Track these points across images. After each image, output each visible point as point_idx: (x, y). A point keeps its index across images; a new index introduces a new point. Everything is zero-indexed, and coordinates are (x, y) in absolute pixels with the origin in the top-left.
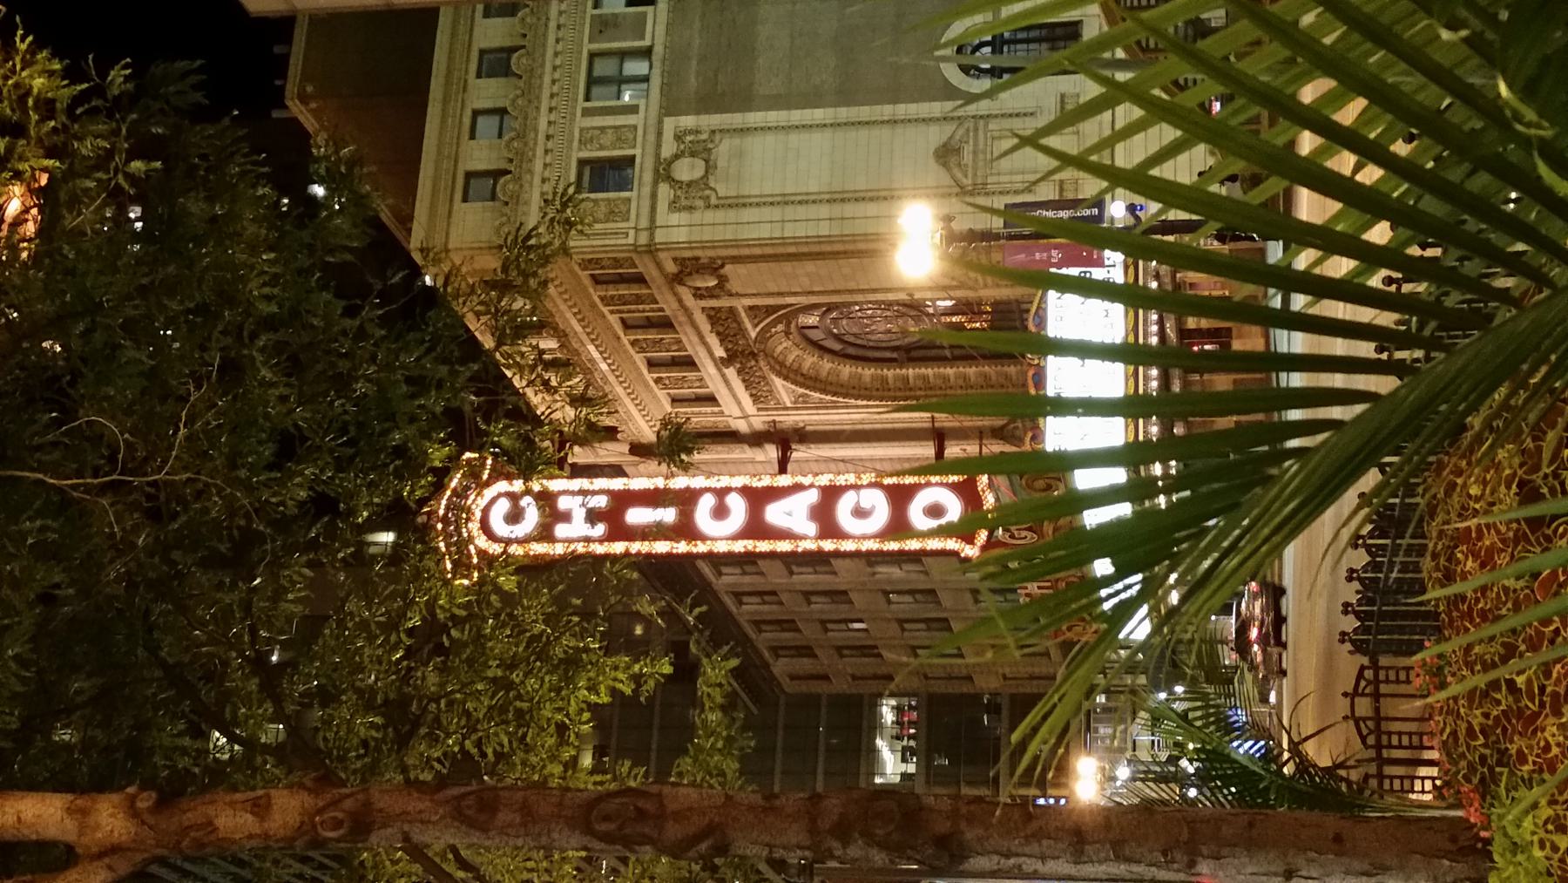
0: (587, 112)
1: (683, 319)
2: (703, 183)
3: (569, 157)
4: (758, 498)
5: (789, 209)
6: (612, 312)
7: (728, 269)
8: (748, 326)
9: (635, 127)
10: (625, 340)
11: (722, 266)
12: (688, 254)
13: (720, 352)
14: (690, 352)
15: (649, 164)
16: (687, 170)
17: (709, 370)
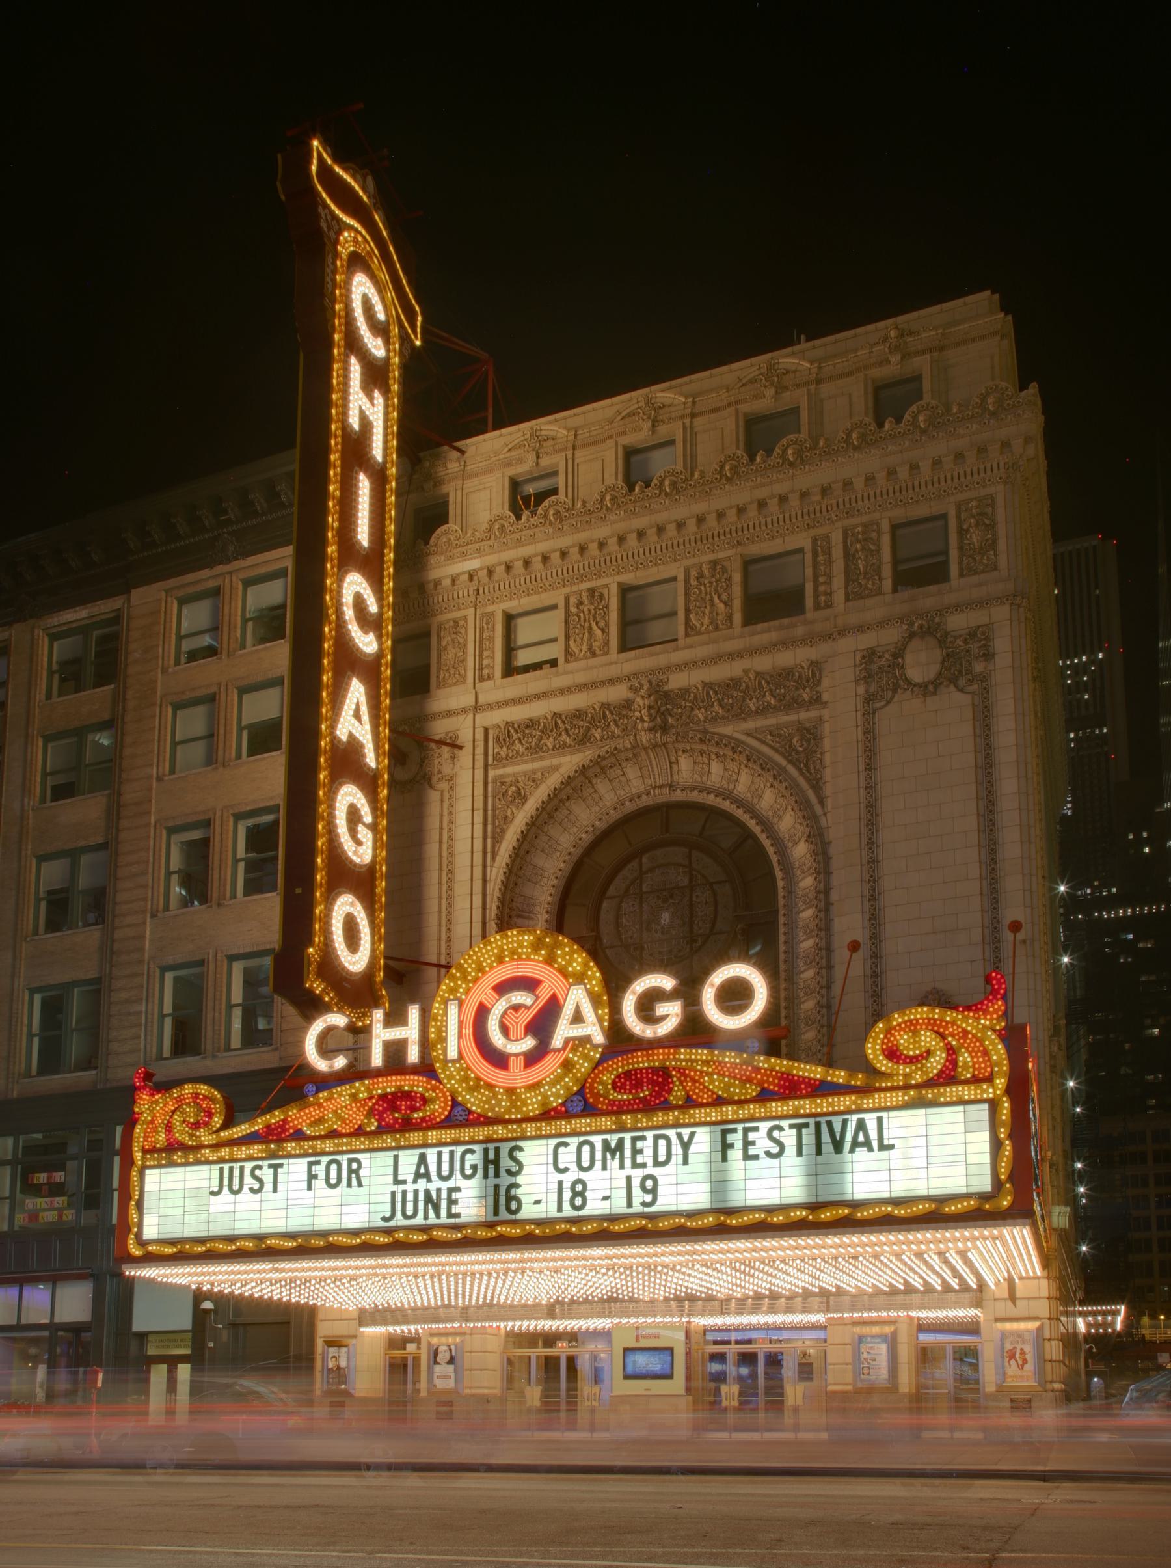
6: (821, 546)
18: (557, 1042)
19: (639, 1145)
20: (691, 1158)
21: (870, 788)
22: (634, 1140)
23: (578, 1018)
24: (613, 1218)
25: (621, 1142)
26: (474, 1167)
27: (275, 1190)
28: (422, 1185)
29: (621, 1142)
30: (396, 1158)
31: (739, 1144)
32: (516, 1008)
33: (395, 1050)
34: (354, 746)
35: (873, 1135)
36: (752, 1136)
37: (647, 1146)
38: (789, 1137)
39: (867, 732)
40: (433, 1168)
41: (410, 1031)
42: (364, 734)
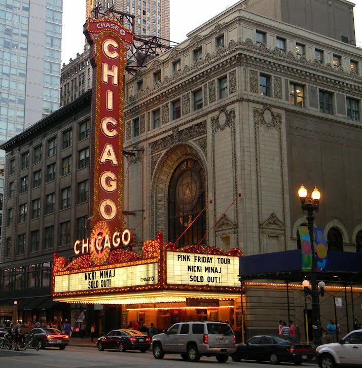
0: (286, 80)
1: (201, 113)
2: (263, 122)
3: (272, 71)
4: (114, 141)
5: (254, 154)
7: (228, 130)
8: (194, 139)
9: (281, 98)
10: (190, 91)
12: (237, 113)
13: (181, 128)
14: (181, 118)
15: (270, 103)
16: (268, 117)
17: (172, 123)
18: (105, 247)
23: (107, 242)
34: (109, 162)
41: (87, 245)
42: (113, 157)
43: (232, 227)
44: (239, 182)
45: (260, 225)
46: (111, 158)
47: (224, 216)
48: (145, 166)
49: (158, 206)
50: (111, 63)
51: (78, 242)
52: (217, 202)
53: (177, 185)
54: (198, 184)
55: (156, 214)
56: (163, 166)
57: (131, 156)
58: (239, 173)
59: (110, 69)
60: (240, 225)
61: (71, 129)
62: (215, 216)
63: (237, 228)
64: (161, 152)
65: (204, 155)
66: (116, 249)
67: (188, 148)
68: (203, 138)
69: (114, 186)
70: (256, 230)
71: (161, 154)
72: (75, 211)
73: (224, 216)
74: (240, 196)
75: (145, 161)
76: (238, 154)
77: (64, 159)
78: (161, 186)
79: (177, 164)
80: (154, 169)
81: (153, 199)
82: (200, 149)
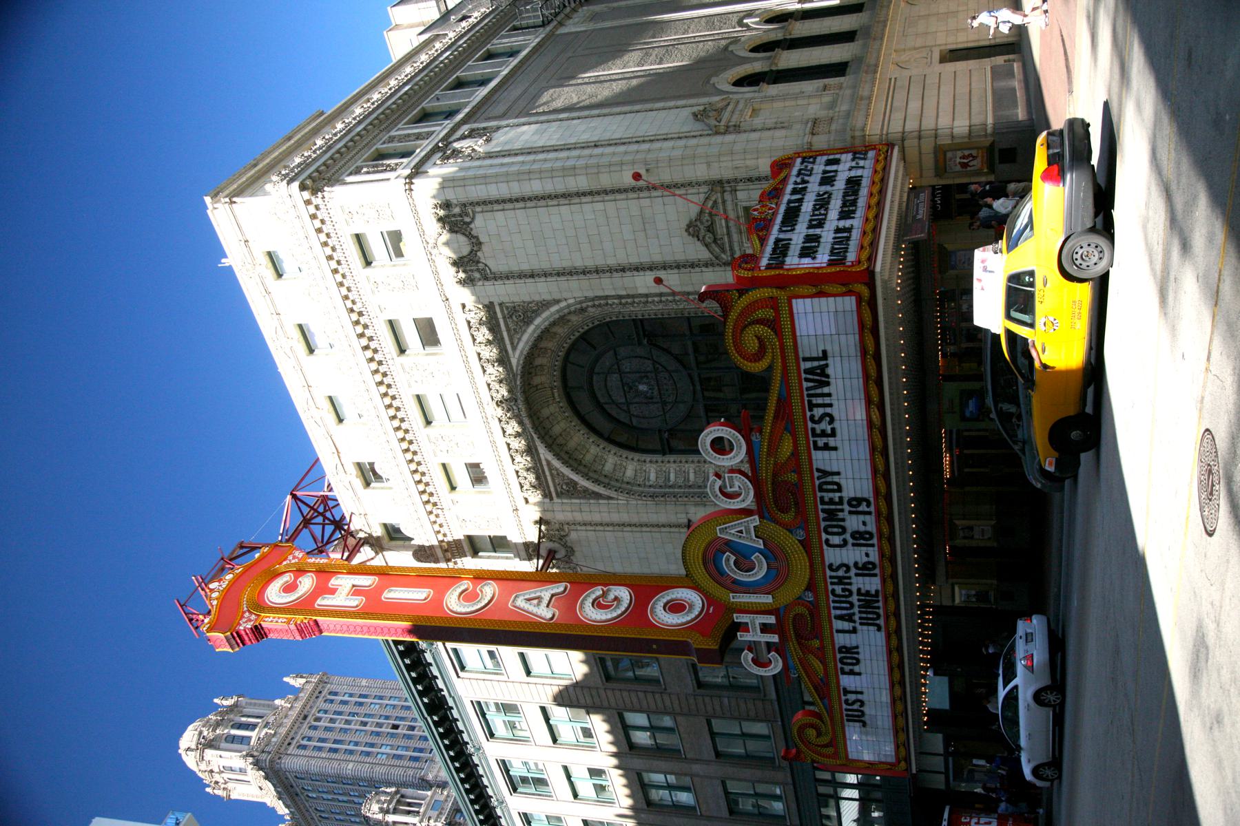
8: (509, 347)
11: (473, 219)
19: (826, 499)
20: (835, 470)
21: (546, 274)
22: (823, 502)
24: (878, 513)
25: (823, 511)
26: (843, 590)
27: (861, 693)
28: (856, 617)
29: (823, 511)
30: (838, 631)
31: (825, 440)
32: (735, 563)
33: (765, 628)
35: (816, 364)
36: (818, 432)
37: (827, 496)
38: (818, 412)
39: (508, 278)
40: (844, 612)
43: (720, 201)
44: (606, 181)
45: (717, 133)
46: (546, 595)
47: (692, 229)
48: (578, 517)
49: (680, 481)
50: (323, 589)
51: (747, 656)
52: (657, 258)
53: (627, 421)
54: (622, 352)
55: (700, 487)
56: (580, 463)
57: (553, 558)
58: (582, 183)
59: (333, 591)
60: (715, 174)
61: (504, 766)
62: (693, 266)
63: (720, 182)
64: (544, 463)
65: (545, 315)
66: (758, 496)
67: (537, 380)
68: (504, 318)
69: (624, 594)
70: (729, 138)
71: (548, 463)
72: (696, 761)
73: (692, 229)
74: (637, 176)
75: (569, 517)
76: (536, 187)
77: (576, 796)
78: (630, 473)
79: (576, 421)
80: (586, 490)
81: (661, 493)
82: (532, 328)
